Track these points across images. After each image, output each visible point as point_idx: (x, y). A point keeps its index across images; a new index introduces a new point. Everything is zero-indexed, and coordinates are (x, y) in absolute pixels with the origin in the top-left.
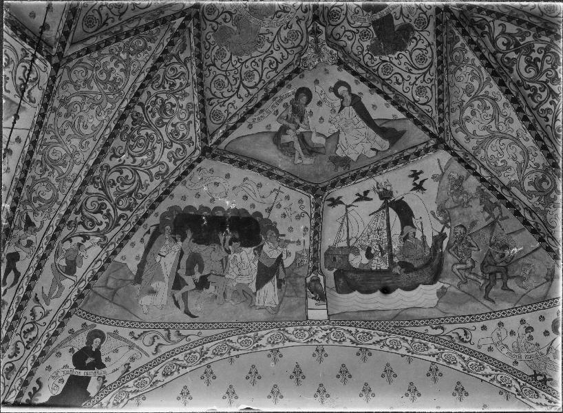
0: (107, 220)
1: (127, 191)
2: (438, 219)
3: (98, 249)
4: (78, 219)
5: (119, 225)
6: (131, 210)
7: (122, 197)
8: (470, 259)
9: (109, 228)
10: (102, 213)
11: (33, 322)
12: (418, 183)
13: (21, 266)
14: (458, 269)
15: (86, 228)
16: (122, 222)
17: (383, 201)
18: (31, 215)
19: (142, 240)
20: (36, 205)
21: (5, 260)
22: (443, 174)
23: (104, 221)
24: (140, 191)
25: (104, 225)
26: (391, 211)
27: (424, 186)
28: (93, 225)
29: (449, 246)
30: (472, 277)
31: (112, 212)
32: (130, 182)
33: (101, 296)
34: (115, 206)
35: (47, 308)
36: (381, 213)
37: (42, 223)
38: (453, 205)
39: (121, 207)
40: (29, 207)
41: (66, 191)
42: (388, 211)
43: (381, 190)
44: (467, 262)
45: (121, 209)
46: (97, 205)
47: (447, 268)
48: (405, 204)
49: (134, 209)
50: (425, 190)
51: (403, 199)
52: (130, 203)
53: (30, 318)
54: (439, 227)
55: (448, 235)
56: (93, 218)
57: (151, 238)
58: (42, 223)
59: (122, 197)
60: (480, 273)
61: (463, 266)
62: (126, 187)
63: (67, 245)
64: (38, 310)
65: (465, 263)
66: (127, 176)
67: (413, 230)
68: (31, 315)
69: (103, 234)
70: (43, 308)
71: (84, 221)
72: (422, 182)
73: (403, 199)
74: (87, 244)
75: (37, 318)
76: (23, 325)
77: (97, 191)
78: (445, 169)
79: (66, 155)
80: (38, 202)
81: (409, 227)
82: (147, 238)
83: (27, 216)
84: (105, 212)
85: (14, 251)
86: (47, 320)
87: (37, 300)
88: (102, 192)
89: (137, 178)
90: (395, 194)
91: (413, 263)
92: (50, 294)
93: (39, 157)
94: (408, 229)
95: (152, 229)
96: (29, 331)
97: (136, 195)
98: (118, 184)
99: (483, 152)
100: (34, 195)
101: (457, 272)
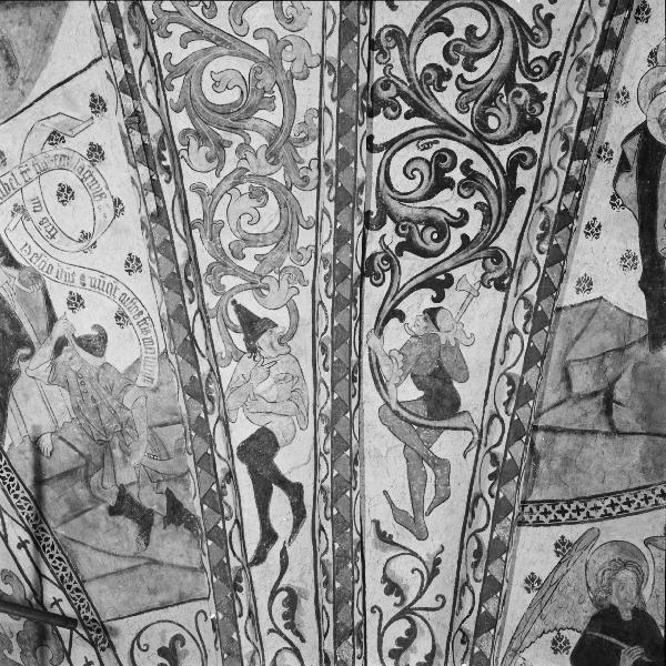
0: (478, 197)
1: (495, 75)
3: (492, 298)
4: (387, 242)
5: (522, 191)
6: (535, 127)
7: (490, 102)
9: (495, 221)
10: (450, 184)
11: (406, 613)
13: (293, 461)
15: (424, 254)
16: (525, 178)
18: (248, 300)
19: (615, 200)
20: (249, 264)
21: (242, 470)
23: (468, 205)
24: (534, 52)
25: (476, 218)
28: (442, 233)
31: (480, 166)
32: (489, 40)
33: (570, 431)
34: (481, 138)
35: (426, 549)
37: (294, 311)
39: (500, 134)
40: (229, 282)
41: (313, 174)
45: (502, 142)
46: (424, 167)
49: (543, 118)
52: (520, 109)
53: (389, 605)
56: (432, 213)
57: (641, 176)
58: (294, 311)
59: (490, 102)
62: (483, 65)
63: (396, 335)
64: (403, 569)
66: (471, 30)
68: (388, 592)
69: (485, 247)
70: (413, 554)
71: (409, 237)
74: (453, 297)
75: (411, 596)
76: (381, 636)
77: (402, 125)
79: (255, 72)
80: (250, 252)
82: (628, 186)
83: (239, 309)
84: (457, 175)
85: (252, 429)
86: (443, 584)
87: (384, 538)
88: (418, 122)
89: (504, 18)
92: (416, 505)
93: (181, 122)
95: (633, 145)
96: (405, 643)
97: (528, 71)
98: (457, 70)
100: (227, 238)
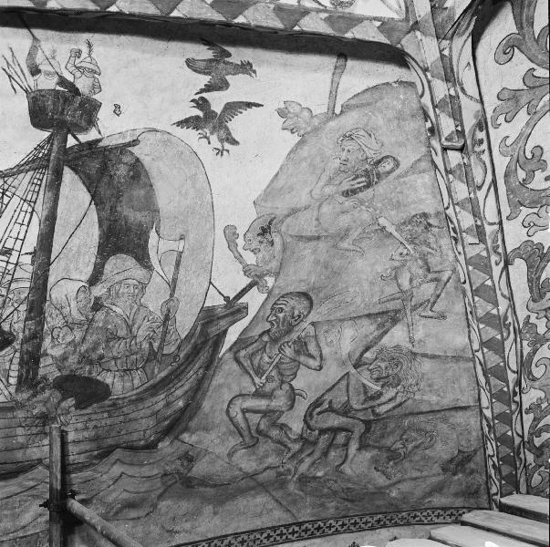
2: (239, 258)
8: (286, 387)
12: (217, 107)
14: (244, 411)
17: (46, 134)
22: (332, 114)
26: (74, 192)
27: (237, 125)
29: (241, 343)
30: (275, 433)
36: (24, 180)
38: (310, 230)
42: (55, 184)
43: (47, 83)
44: (279, 392)
47: (213, 405)
48: (138, 172)
50: (235, 142)
51: (135, 150)
54: (230, 280)
55: (252, 312)
60: (297, 426)
61: (262, 404)
65: (269, 396)
67: (139, 273)
72: (232, 108)
73: (135, 150)
78: (346, 108)
81: (130, 262)
90: (104, 115)
91: (109, 381)
94: (120, 265)
99: (523, 117)
101: (239, 417)
